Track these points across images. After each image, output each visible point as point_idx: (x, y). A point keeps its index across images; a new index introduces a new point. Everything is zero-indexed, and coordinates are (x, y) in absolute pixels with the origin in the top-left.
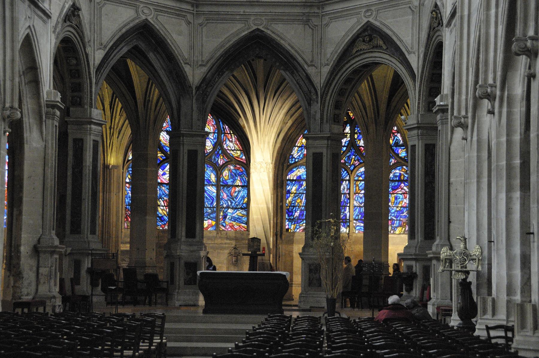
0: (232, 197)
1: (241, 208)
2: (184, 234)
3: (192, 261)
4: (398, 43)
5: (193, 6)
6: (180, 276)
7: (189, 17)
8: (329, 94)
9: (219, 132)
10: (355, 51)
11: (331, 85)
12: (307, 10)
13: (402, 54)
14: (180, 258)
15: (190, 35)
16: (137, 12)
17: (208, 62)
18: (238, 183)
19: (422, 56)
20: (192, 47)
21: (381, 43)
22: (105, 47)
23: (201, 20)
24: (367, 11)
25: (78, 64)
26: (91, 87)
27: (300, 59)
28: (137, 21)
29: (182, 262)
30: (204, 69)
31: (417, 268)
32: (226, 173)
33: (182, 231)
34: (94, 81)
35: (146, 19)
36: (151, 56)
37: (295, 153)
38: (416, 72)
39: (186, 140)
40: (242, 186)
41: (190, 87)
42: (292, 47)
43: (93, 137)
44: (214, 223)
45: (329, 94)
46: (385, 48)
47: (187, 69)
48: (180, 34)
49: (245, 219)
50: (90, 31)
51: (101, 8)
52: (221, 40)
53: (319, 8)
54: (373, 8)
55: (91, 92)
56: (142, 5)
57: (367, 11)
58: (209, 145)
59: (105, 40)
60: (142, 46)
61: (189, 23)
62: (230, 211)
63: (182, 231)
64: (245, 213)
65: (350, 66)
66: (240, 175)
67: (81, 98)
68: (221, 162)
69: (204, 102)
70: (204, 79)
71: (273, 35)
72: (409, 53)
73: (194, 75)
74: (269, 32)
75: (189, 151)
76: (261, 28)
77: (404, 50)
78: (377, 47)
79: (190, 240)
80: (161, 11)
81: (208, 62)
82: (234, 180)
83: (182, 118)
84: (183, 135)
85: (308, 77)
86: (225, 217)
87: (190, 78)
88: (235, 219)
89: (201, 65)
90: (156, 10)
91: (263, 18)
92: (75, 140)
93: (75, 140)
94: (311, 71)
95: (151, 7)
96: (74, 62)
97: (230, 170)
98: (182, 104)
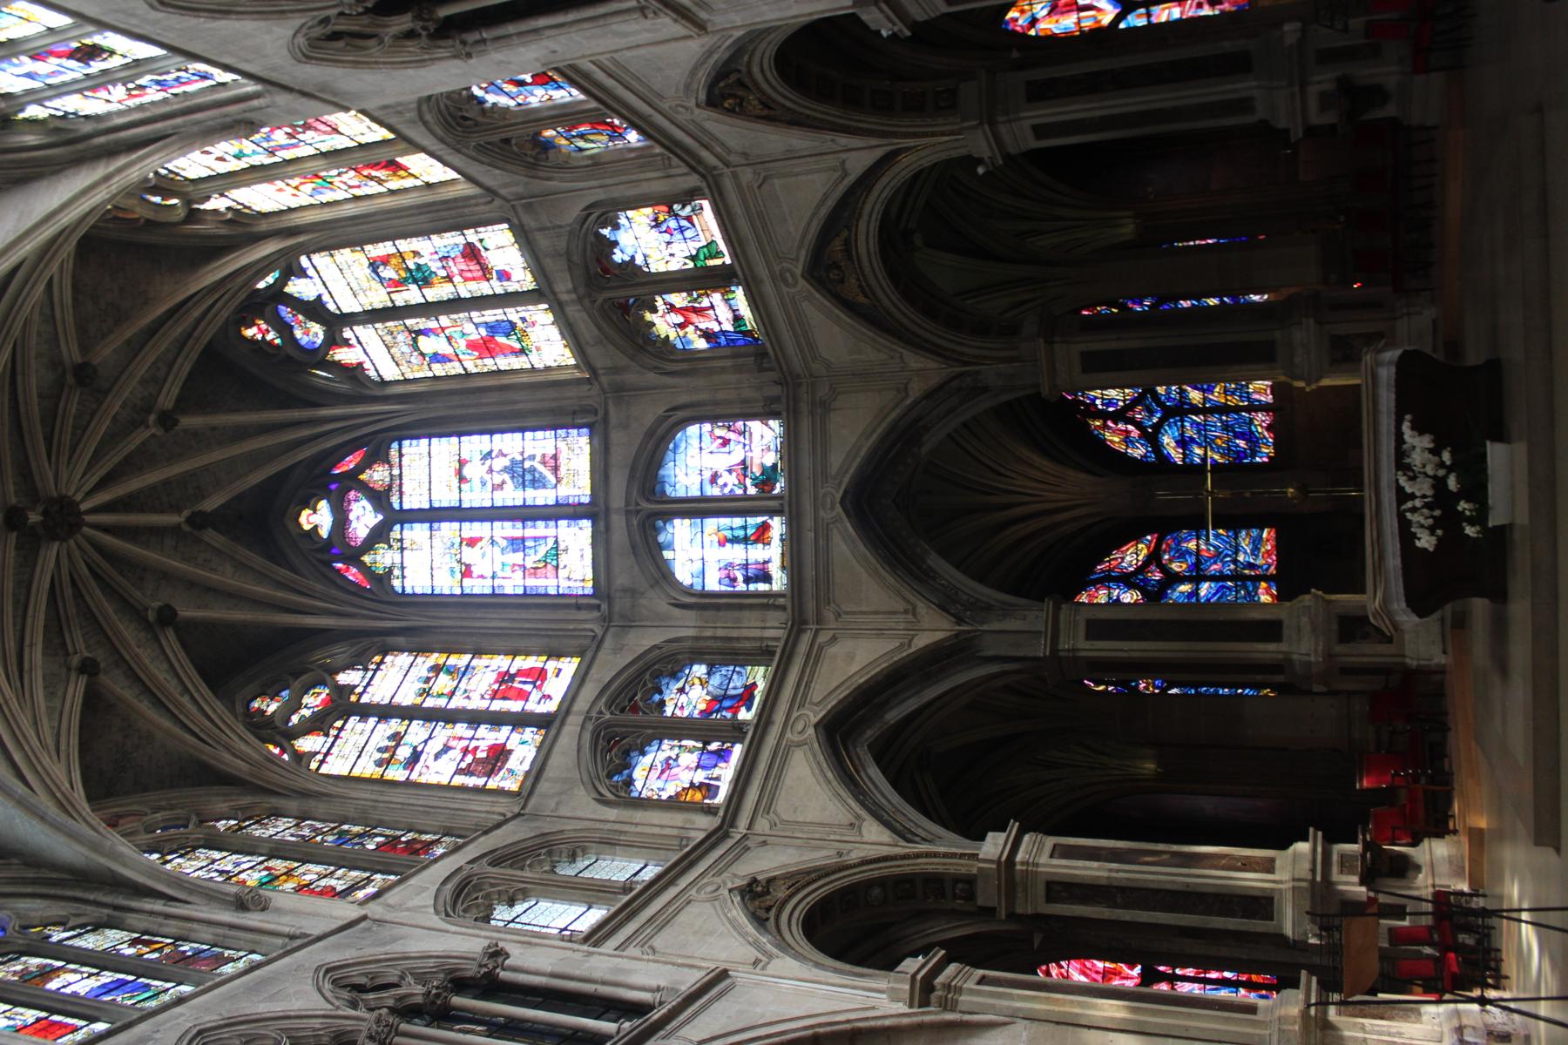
0: (1218, 556)
1: (1236, 538)
2: (1272, 647)
3: (1335, 627)
4: (831, 203)
5: (801, 631)
6: (1365, 652)
7: (823, 637)
8: (958, 348)
9: (1107, 579)
10: (861, 299)
11: (939, 346)
12: (804, 407)
13: (851, 192)
14: (1329, 656)
15: (855, 637)
16: (799, 745)
17: (909, 602)
18: (1192, 545)
19: (844, 141)
20: (880, 632)
21: (837, 245)
22: (858, 817)
23: (829, 614)
24: (787, 285)
25: (881, 882)
26: (935, 855)
27: (894, 415)
28: (816, 745)
29: (1339, 649)
30: (922, 608)
31: (1323, 80)
32: (1175, 567)
33: (1266, 650)
34: (923, 847)
35: (816, 726)
36: (893, 716)
37: (1138, 452)
38: (879, 153)
39: (1065, 644)
40: (1198, 538)
41: (956, 636)
42: (874, 431)
43: (1044, 859)
44: (1263, 585)
45: (958, 348)
46: (845, 234)
47: (922, 641)
48: (850, 657)
49: (1255, 532)
50: (822, 848)
51: (783, 822)
52: (865, 575)
53: (800, 385)
54: (777, 269)
55: (945, 855)
56: (788, 735)
57: (785, 281)
58: (1129, 597)
59: (844, 817)
60: (870, 734)
61: (834, 639)
62: (1241, 558)
63: (1266, 650)
64: (1243, 533)
65: (896, 306)
66: (1179, 544)
67: (958, 879)
68: (1158, 576)
69: (989, 608)
70: (942, 608)
71: (851, 471)
72: (845, 174)
73: (933, 630)
74: (846, 480)
75: (1088, 637)
76: (838, 496)
77: (842, 188)
78: (847, 251)
79: (1286, 632)
80: (805, 695)
81: (909, 602)
82: (1188, 552)
83: (1021, 653)
84: (1054, 649)
85: (929, 395)
86: (1251, 566)
87: (939, 636)
88: (1255, 551)
89: (914, 615)
90: (802, 706)
91: (821, 492)
92: (1050, 899)
93: (1050, 899)
94: (916, 389)
95: (795, 714)
96: (876, 891)
97: (1171, 561)
98: (991, 653)
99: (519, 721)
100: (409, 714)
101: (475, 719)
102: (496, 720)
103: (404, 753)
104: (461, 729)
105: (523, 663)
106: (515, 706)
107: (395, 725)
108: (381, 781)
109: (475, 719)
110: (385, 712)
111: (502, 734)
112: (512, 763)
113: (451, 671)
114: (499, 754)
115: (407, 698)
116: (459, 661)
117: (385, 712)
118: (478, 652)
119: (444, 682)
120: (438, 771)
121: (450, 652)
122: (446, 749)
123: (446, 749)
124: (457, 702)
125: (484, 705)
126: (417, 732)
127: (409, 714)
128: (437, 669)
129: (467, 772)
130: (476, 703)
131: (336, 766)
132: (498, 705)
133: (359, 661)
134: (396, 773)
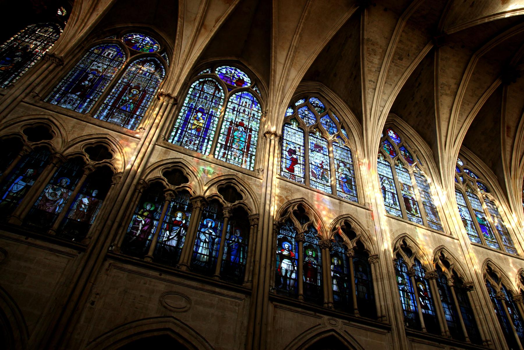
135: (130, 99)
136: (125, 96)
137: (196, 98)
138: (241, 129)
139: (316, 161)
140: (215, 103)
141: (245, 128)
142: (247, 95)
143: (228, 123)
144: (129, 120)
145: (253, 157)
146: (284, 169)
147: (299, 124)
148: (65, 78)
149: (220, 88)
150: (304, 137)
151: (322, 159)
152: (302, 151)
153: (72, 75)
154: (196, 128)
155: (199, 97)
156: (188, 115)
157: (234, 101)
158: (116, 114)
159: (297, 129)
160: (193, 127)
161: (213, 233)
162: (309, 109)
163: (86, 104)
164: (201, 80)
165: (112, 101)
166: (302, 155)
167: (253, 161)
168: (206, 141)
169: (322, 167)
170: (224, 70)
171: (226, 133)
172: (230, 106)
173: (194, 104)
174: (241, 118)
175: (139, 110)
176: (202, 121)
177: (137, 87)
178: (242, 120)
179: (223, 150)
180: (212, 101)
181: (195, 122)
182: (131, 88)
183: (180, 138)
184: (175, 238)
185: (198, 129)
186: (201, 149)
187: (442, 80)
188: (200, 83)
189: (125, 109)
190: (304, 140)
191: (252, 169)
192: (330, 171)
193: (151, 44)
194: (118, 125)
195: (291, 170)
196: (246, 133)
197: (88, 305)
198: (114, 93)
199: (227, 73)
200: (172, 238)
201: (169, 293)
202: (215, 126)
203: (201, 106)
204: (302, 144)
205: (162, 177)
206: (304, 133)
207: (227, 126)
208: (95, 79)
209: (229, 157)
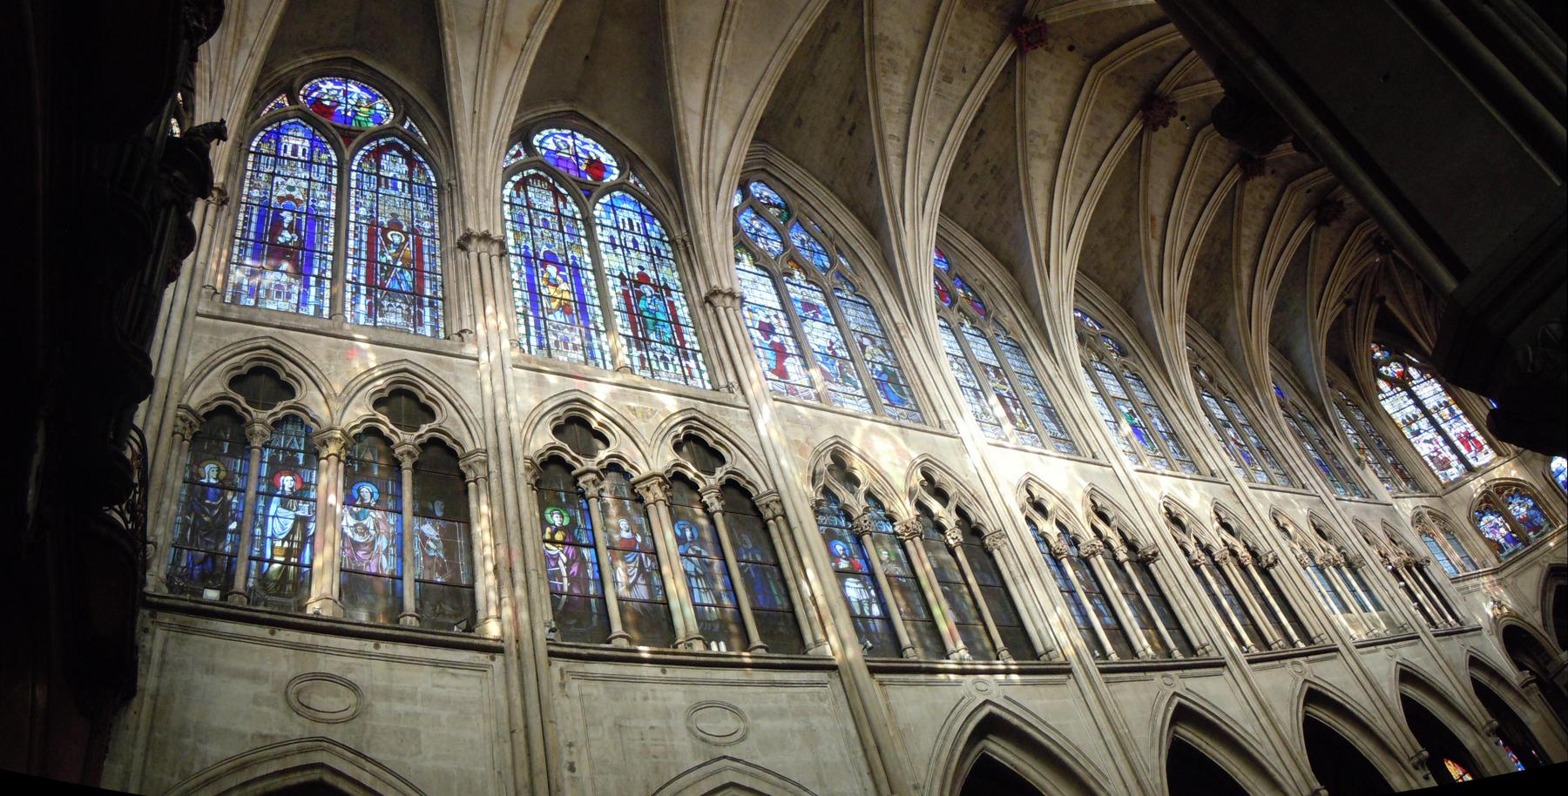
99: (1462, 459)
100: (1427, 413)
101: (1448, 441)
102: (1455, 450)
103: (1414, 427)
104: (1440, 439)
105: (1475, 434)
106: (1464, 451)
107: (1418, 412)
108: (1400, 430)
109: (1448, 441)
110: (1419, 403)
111: (1453, 457)
112: (1449, 472)
113: (1452, 411)
114: (1445, 465)
115: (1430, 404)
116: (1459, 412)
117: (1419, 403)
118: (1466, 414)
119: (1446, 412)
120: (1424, 450)
121: (1457, 402)
122: (1430, 442)
123: (1430, 442)
124: (1444, 426)
125: (1454, 438)
126: (1424, 423)
127: (1427, 413)
128: (1447, 405)
129: (1432, 458)
130: (1452, 435)
131: (1387, 406)
132: (1458, 443)
133: (1422, 370)
134: (1407, 432)
135: (396, 260)
136: (382, 254)
137: (527, 229)
138: (647, 290)
139: (819, 342)
140: (571, 235)
141: (654, 286)
142: (624, 199)
143: (618, 281)
144: (420, 315)
145: (699, 356)
146: (770, 375)
147: (753, 256)
148: (239, 234)
149: (563, 191)
150: (775, 286)
151: (828, 335)
152: (784, 324)
153: (247, 222)
154: (560, 305)
155: (531, 225)
156: (530, 277)
157: (605, 222)
158: (386, 303)
159: (754, 269)
160: (554, 305)
161: (704, 553)
162: (759, 215)
163: (313, 290)
164: (516, 178)
165: (363, 271)
166: (787, 332)
167: (703, 367)
168: (593, 333)
169: (834, 355)
170: (550, 140)
171: (623, 308)
172: (603, 235)
173: (529, 244)
174: (636, 263)
175: (427, 283)
176: (564, 286)
177: (395, 225)
178: (641, 268)
179: (636, 353)
180: (561, 230)
181: (552, 290)
182: (385, 231)
183: (540, 338)
184: (640, 581)
185: (565, 309)
186: (593, 358)
187: (1032, 125)
188: (517, 186)
189: (396, 287)
190: (778, 294)
191: (709, 387)
192: (852, 360)
193: (369, 101)
194: (401, 331)
195: (782, 373)
196: (661, 298)
197: (566, 773)
198: (355, 250)
199: (559, 150)
200: (635, 582)
201: (698, 707)
202: (595, 294)
203: (545, 248)
204: (778, 306)
205: (558, 443)
206: (771, 277)
207: (619, 290)
208: (299, 221)
209: (654, 366)
